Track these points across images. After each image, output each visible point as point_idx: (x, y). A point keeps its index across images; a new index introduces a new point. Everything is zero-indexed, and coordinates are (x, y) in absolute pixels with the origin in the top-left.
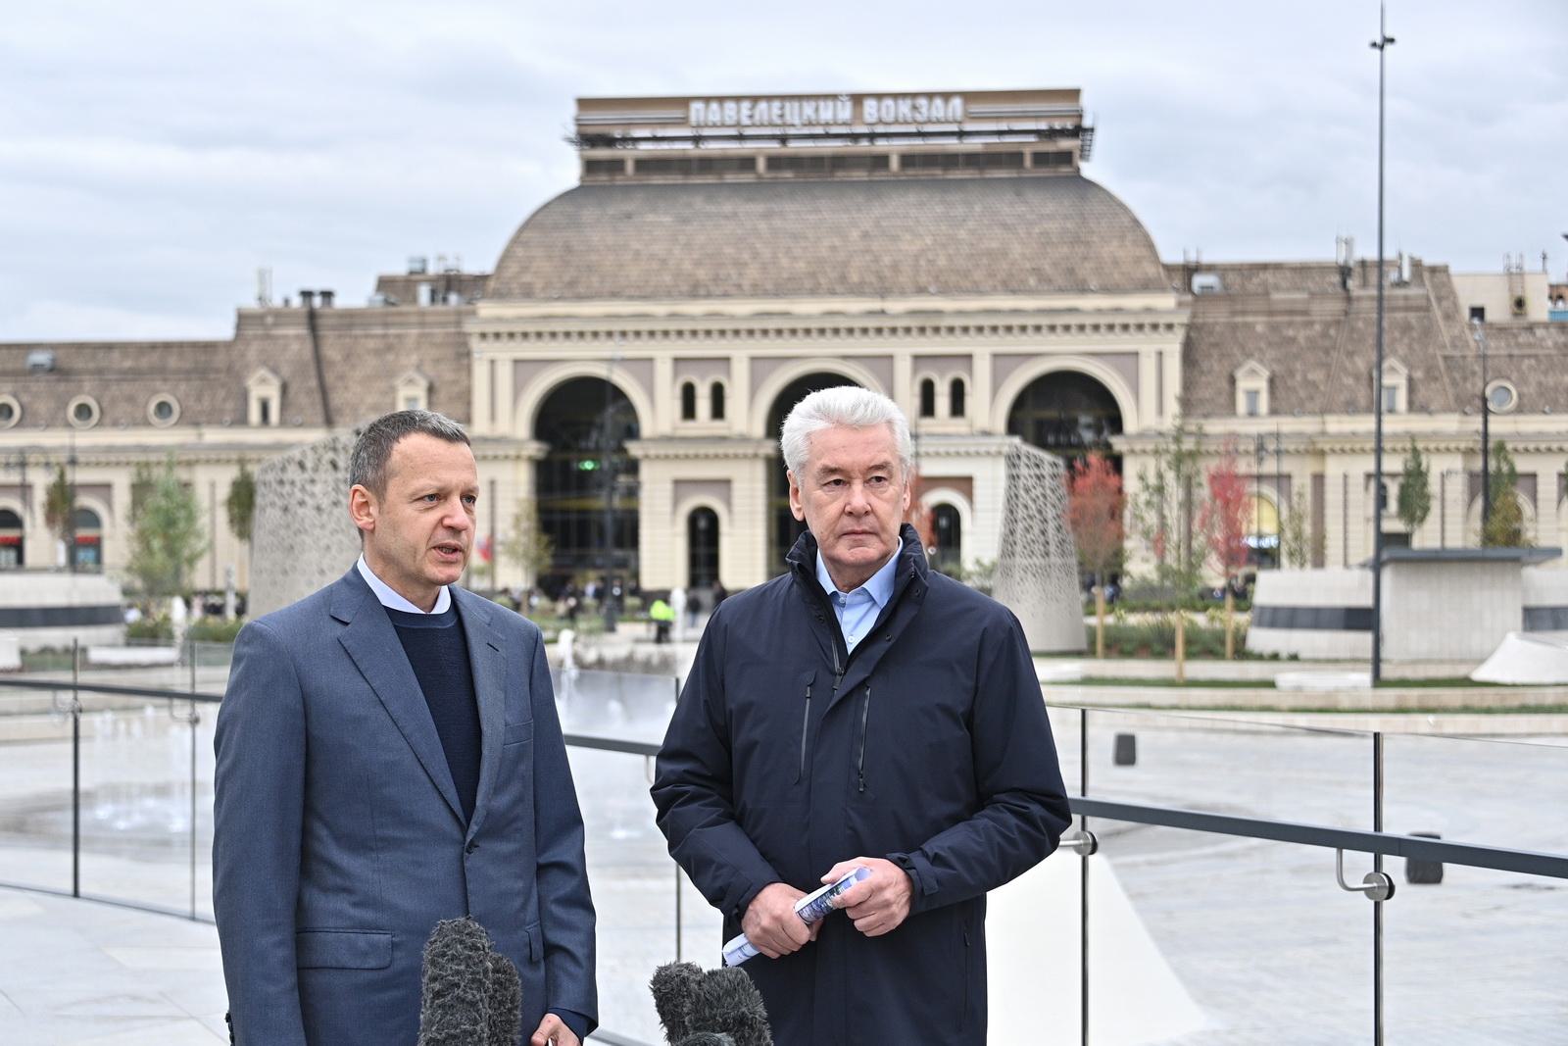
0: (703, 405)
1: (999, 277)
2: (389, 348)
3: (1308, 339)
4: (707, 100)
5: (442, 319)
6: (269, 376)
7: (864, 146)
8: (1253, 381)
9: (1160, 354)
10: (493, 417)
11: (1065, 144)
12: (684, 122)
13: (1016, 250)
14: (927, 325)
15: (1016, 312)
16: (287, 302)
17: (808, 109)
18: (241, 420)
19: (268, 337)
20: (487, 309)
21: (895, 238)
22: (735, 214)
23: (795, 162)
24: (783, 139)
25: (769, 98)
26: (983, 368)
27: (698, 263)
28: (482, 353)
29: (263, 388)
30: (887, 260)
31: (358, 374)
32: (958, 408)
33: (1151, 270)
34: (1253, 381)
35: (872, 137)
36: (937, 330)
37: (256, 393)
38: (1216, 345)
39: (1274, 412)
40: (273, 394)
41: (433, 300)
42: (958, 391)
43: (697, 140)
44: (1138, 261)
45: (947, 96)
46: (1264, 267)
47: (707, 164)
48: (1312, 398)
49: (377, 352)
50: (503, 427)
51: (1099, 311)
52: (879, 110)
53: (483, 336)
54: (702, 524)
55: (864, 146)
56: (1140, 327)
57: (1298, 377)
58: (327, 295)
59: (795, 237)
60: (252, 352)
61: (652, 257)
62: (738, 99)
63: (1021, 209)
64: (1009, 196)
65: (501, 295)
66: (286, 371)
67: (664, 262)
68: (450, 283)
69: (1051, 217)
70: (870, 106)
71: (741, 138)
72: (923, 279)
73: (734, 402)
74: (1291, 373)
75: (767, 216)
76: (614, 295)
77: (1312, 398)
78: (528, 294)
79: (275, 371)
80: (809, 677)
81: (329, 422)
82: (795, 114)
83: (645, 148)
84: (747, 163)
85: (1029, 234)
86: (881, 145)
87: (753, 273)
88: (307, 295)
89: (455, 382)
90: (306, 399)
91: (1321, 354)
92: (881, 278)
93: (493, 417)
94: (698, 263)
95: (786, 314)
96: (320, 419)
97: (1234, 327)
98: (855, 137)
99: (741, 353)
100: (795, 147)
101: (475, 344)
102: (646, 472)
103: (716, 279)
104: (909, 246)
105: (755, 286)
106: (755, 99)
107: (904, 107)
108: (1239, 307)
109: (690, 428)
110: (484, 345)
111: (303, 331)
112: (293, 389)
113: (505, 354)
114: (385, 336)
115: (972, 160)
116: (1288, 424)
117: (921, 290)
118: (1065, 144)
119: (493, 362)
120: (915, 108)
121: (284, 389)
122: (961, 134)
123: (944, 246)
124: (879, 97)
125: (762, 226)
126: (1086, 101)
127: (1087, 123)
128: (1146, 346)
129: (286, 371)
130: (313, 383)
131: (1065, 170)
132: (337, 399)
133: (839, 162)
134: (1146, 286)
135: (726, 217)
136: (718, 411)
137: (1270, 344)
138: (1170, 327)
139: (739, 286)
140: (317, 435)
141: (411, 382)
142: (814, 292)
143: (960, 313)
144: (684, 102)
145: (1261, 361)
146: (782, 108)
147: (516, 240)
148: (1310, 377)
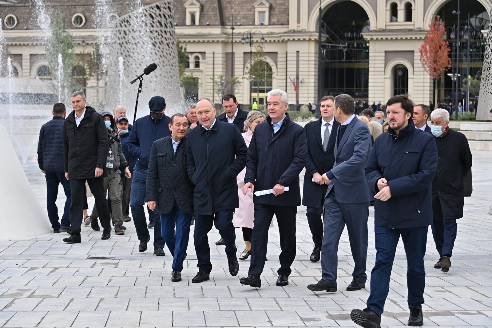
0: (401, 14)
10: (299, 22)
18: (182, 24)
40: (197, 10)
50: (303, 26)
54: (400, 73)
73: (417, 13)
80: (268, 138)
81: (223, 24)
90: (213, 14)
93: (299, 22)
96: (218, 23)
109: (394, 26)
112: (206, 8)
130: (216, 5)
136: (409, 17)
140: (217, 31)
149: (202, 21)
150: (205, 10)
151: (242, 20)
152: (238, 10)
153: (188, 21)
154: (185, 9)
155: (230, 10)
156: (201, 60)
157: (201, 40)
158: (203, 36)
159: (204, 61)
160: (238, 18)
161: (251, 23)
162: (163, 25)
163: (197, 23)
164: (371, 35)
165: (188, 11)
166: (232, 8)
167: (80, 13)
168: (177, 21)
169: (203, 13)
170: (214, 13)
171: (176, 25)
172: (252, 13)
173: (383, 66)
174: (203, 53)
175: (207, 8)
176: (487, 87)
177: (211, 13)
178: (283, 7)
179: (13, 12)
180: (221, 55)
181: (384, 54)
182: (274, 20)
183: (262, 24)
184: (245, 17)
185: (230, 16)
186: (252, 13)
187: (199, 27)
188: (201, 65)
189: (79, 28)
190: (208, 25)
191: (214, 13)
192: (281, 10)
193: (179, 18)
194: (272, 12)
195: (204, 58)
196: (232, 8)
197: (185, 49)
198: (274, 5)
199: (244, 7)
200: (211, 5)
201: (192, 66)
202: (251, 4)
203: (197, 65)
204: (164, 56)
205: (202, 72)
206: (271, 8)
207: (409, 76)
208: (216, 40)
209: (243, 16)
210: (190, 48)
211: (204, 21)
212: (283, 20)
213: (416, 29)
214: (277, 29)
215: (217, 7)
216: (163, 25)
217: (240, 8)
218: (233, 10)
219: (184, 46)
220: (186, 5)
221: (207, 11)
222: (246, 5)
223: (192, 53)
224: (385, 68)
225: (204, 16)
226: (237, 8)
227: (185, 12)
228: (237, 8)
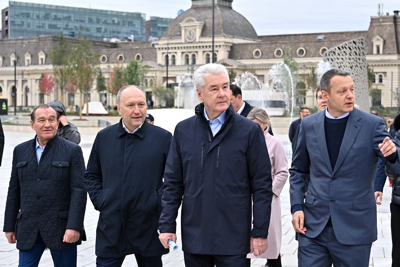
16: (388, 14)
18: (371, 53)
19: (381, 25)
29: (378, 42)
37: (375, 43)
40: (381, 44)
60: (375, 31)
66: (385, 37)
79: (382, 37)
96: (396, 52)
111: (392, 23)
112: (387, 42)
121: (385, 42)
130: (394, 40)
149: (384, 51)
150: (387, 44)
153: (375, 51)
154: (373, 43)
156: (383, 78)
159: (385, 78)
163: (381, 52)
167: (302, 47)
168: (367, 51)
171: (367, 54)
174: (385, 73)
179: (259, 47)
180: (397, 74)
187: (382, 55)
188: (383, 81)
189: (302, 57)
193: (368, 50)
195: (385, 76)
197: (373, 70)
201: (377, 81)
203: (381, 81)
205: (384, 85)
210: (376, 70)
219: (372, 68)
220: (374, 41)
221: (388, 44)
223: (377, 73)
227: (373, 45)
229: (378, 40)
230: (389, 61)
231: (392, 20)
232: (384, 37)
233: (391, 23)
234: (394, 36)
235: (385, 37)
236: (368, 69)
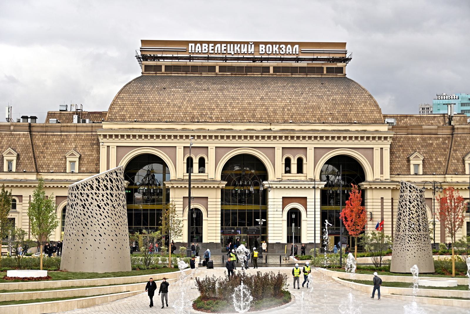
1: (317, 117)
2: (63, 141)
3: (437, 144)
4: (196, 43)
5: (86, 129)
6: (12, 151)
7: (258, 64)
8: (416, 161)
9: (382, 149)
11: (340, 65)
12: (185, 51)
13: (323, 106)
14: (289, 136)
15: (324, 131)
17: (237, 48)
20: (106, 126)
21: (275, 100)
22: (208, 88)
23: (231, 69)
24: (226, 59)
25: (221, 43)
26: (311, 153)
27: (194, 108)
28: (104, 143)
30: (271, 109)
31: (49, 151)
32: (300, 170)
33: (377, 116)
34: (416, 161)
35: (262, 60)
36: (292, 137)
38: (401, 146)
39: (424, 174)
41: (79, 122)
42: (300, 162)
43: (190, 58)
44: (372, 112)
45: (293, 44)
46: (406, 116)
47: (195, 69)
48: (439, 168)
49: (57, 142)
51: (357, 131)
52: (265, 48)
53: (105, 136)
55: (258, 64)
56: (374, 138)
57: (434, 160)
58: (35, 118)
59: (233, 98)
61: (174, 105)
62: (208, 43)
63: (323, 90)
64: (319, 85)
65: (112, 120)
67: (180, 107)
68: (81, 115)
69: (337, 94)
70: (262, 47)
71: (208, 58)
72: (286, 117)
74: (431, 158)
75: (221, 90)
76: (159, 121)
77: (439, 168)
78: (123, 120)
81: (37, 172)
82: (231, 50)
83: (168, 62)
84: (212, 69)
85: (328, 100)
86: (265, 64)
87: (216, 113)
88: (25, 118)
89: (91, 155)
91: (443, 150)
92: (269, 116)
94: (194, 108)
95: (231, 130)
97: (409, 139)
98: (254, 60)
99: (212, 145)
100: (229, 63)
101: (101, 139)
102: (172, 193)
103: (201, 115)
104: (280, 103)
105: (217, 118)
106: (215, 43)
107: (276, 48)
108: (410, 131)
110: (105, 140)
113: (114, 144)
114: (61, 135)
115: (302, 70)
116: (430, 179)
117: (285, 122)
118: (340, 65)
119: (108, 147)
120: (280, 48)
122: (297, 60)
123: (294, 104)
124: (266, 43)
125: (220, 94)
126: (347, 48)
127: (347, 56)
128: (376, 146)
129: (19, 150)
131: (339, 75)
132: (40, 162)
133: (249, 69)
134: (375, 122)
135: (205, 90)
137: (422, 146)
138: (386, 138)
139: (211, 118)
140: (33, 177)
141: (72, 154)
142: (242, 122)
143: (302, 131)
144: (187, 43)
145: (419, 152)
146: (226, 46)
147: (117, 97)
148: (439, 159)
149: (18, 168)
150: (21, 159)
151: (54, 168)
152: (50, 160)
154: (3, 157)
155: (43, 159)
157: (19, 185)
158: (21, 181)
159: (21, 203)
160: (51, 166)
161: (62, 171)
162: (109, 188)
164: (172, 184)
165: (5, 158)
166: (44, 157)
169: (20, 161)
170: (29, 161)
172: (63, 162)
173: (182, 209)
175: (23, 157)
176: (404, 245)
177: (27, 161)
178: (91, 158)
181: (182, 200)
182: (83, 169)
183: (73, 172)
184: (56, 166)
185: (43, 164)
186: (63, 162)
188: (17, 206)
190: (25, 172)
191: (29, 161)
192: (90, 160)
194: (81, 162)
195: (21, 201)
196: (44, 157)
197: (10, 193)
198: (83, 156)
199: (56, 157)
200: (26, 155)
202: (62, 155)
204: (108, 216)
205: (19, 213)
206: (80, 158)
207: (204, 218)
208: (33, 185)
209: (55, 164)
211: (20, 168)
212: (92, 169)
213: (209, 179)
214: (86, 178)
215: (33, 156)
216: (109, 188)
217: (52, 157)
218: (45, 159)
219: (9, 191)
222: (57, 155)
224: (183, 211)
225: (21, 164)
226: (49, 157)
228: (49, 157)
229: (10, 153)
230: (26, 181)
231: (28, 128)
232: (17, 150)
233: (27, 133)
234: (31, 150)
235: (19, 150)
236: (4, 191)
